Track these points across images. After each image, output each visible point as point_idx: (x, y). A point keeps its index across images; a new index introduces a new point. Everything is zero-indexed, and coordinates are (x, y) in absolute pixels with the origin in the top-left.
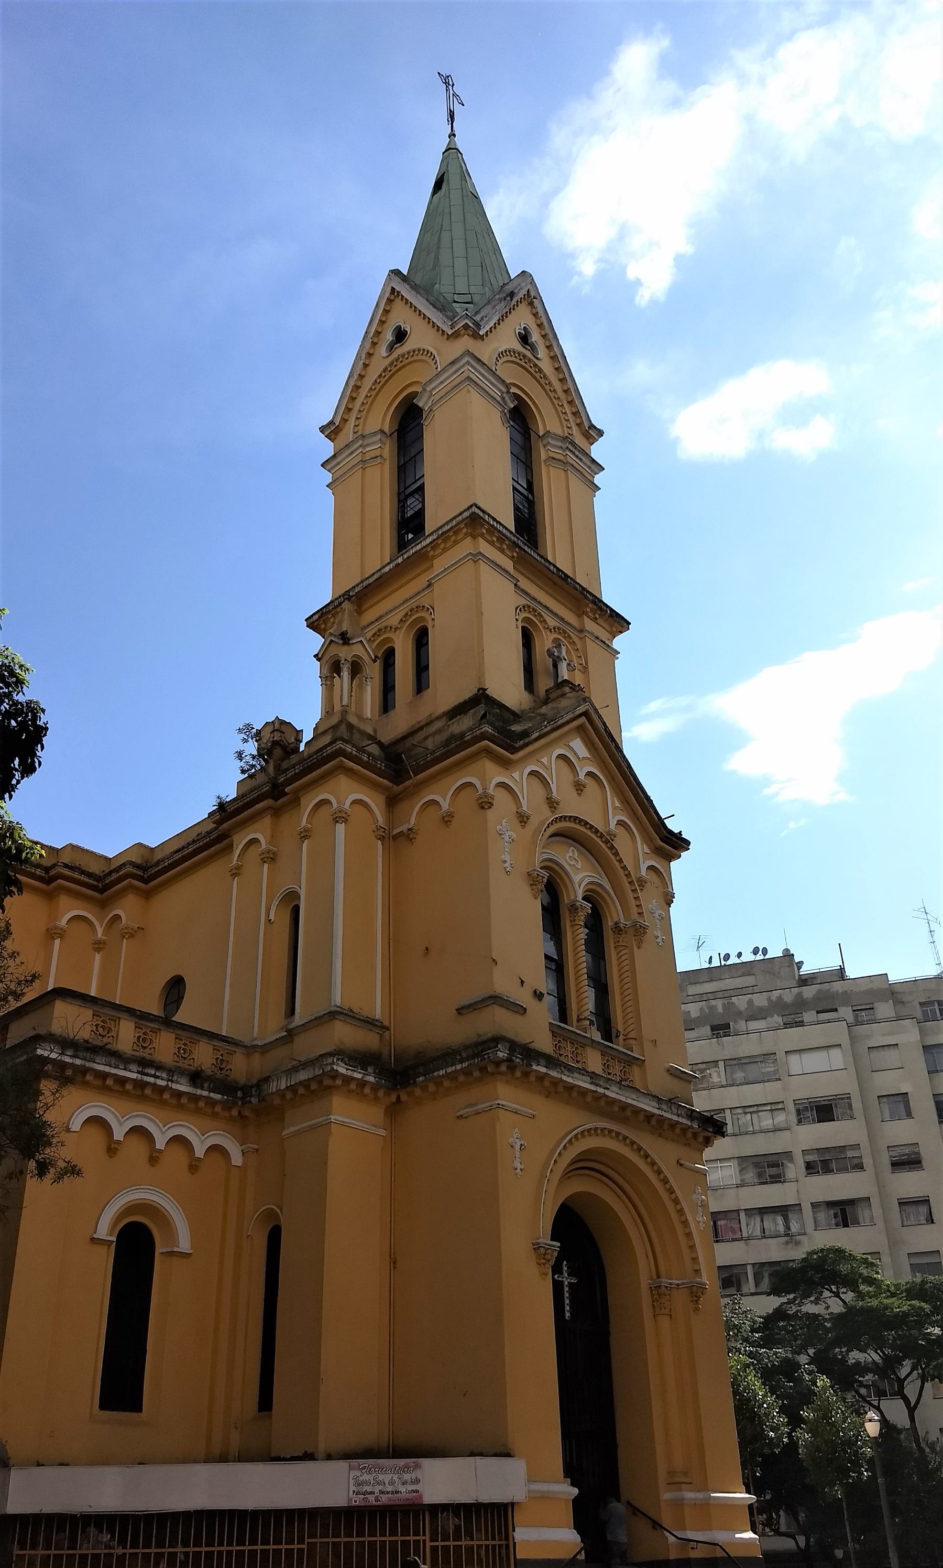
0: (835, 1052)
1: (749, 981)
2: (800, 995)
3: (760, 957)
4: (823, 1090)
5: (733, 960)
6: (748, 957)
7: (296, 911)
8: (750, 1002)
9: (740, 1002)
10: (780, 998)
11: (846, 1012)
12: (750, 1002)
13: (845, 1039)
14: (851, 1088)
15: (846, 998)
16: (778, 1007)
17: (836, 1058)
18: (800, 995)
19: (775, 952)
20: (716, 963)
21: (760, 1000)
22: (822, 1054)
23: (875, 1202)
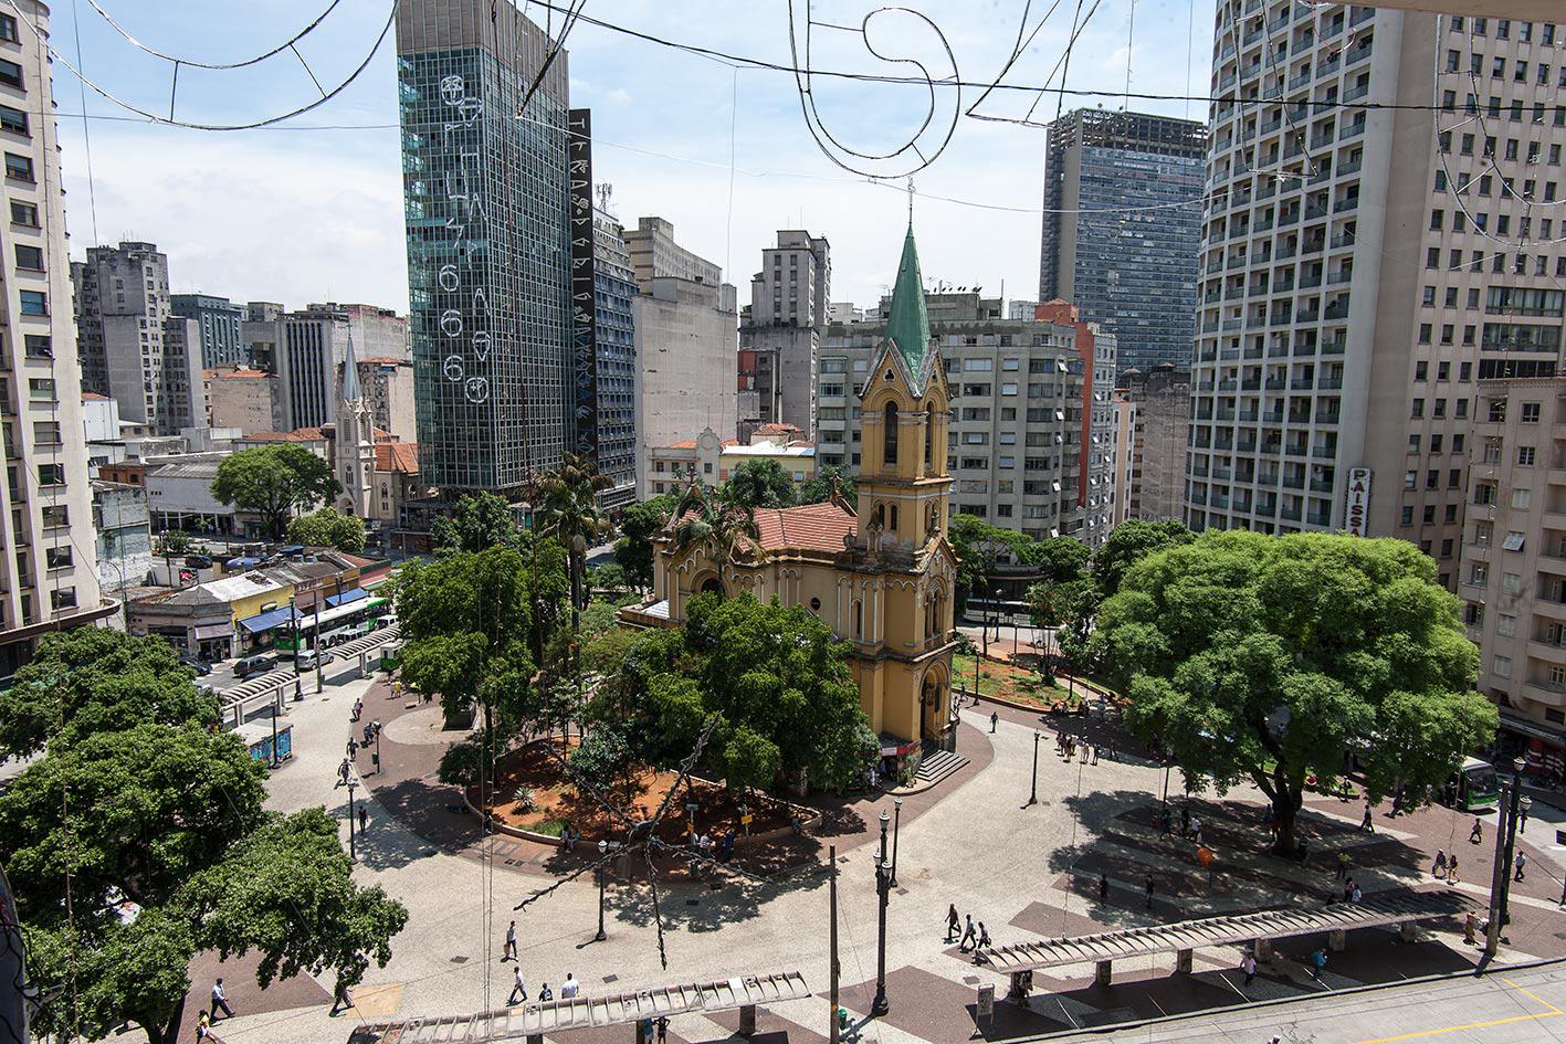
0: (989, 362)
1: (954, 305)
2: (977, 324)
3: (961, 292)
4: (978, 379)
5: (947, 292)
6: (955, 292)
7: (859, 605)
8: (952, 325)
9: (948, 325)
10: (967, 325)
11: (998, 337)
12: (952, 325)
13: (994, 357)
14: (992, 381)
15: (999, 330)
16: (964, 330)
17: (988, 365)
18: (977, 324)
19: (969, 291)
20: (937, 293)
21: (957, 325)
22: (983, 362)
23: (992, 411)
